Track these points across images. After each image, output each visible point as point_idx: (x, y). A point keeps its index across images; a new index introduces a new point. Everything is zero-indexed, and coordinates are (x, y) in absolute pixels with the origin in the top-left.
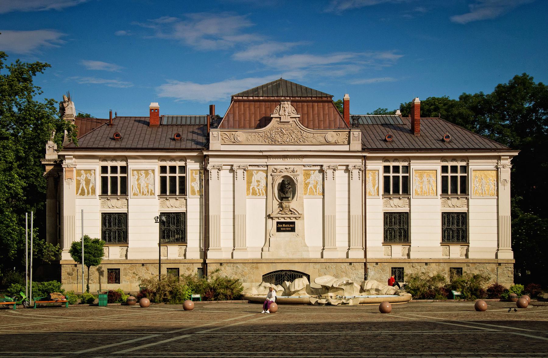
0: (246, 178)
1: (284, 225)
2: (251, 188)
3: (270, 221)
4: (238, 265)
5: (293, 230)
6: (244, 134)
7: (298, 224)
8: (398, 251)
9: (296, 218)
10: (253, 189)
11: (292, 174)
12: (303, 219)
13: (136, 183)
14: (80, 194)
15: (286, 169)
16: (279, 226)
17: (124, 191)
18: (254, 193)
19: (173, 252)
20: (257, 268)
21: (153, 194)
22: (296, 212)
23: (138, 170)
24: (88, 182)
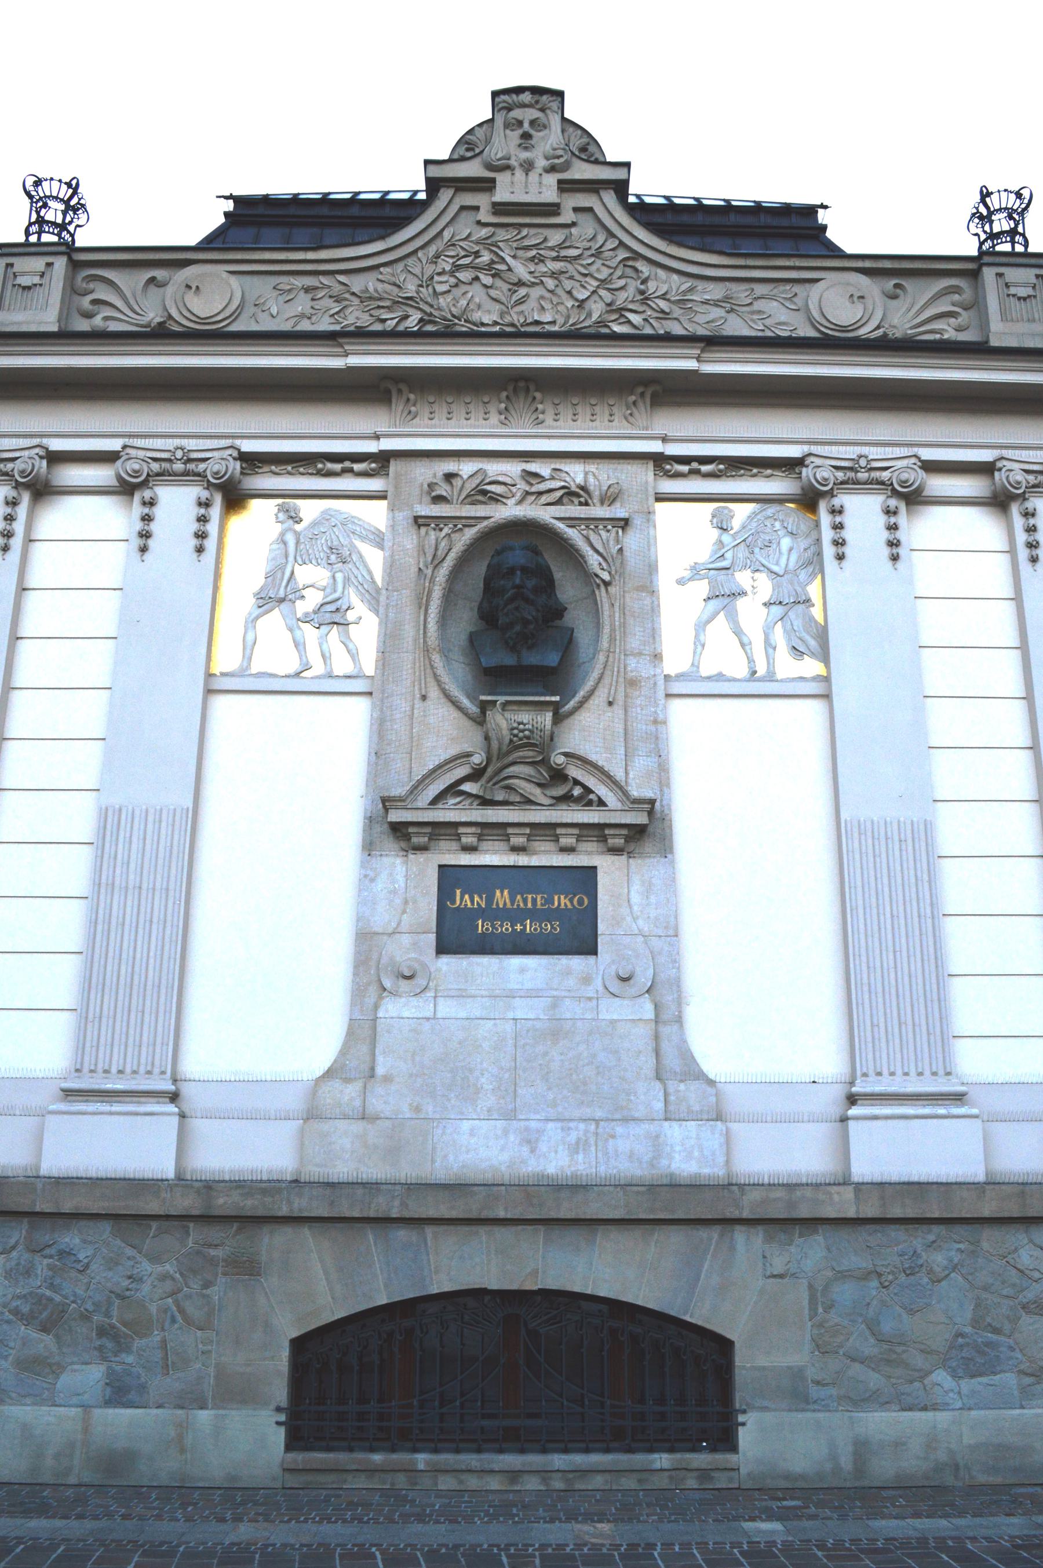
1: (502, 898)
4: (71, 1238)
6: (234, 282)
7: (622, 887)
9: (598, 832)
12: (666, 847)
15: (530, 476)
16: (462, 900)
20: (246, 1268)
22: (602, 790)
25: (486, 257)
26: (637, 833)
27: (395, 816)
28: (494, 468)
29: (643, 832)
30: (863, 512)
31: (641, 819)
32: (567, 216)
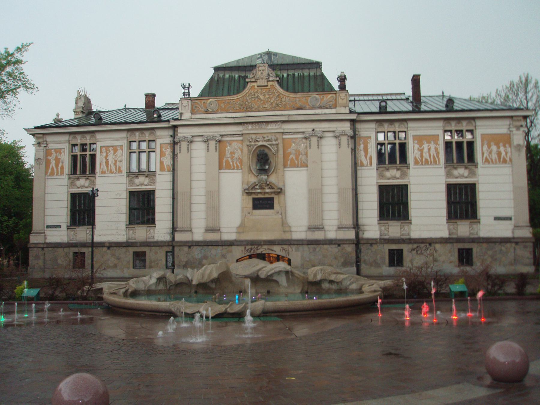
0: (218, 150)
2: (224, 160)
3: (245, 197)
5: (271, 207)
8: (394, 229)
9: (274, 192)
10: (227, 161)
11: (270, 143)
13: (104, 160)
14: (50, 175)
17: (93, 170)
18: (228, 167)
19: (141, 233)
21: (120, 171)
23: (107, 147)
24: (57, 161)
25: (256, 95)
26: (279, 192)
27: (247, 191)
28: (258, 136)
29: (280, 192)
30: (314, 140)
31: (279, 190)
32: (269, 87)
